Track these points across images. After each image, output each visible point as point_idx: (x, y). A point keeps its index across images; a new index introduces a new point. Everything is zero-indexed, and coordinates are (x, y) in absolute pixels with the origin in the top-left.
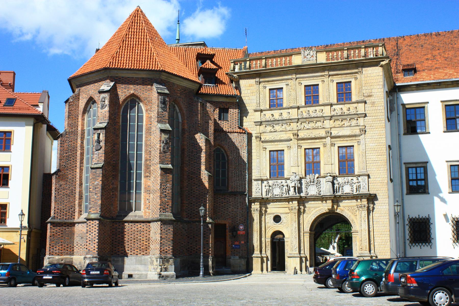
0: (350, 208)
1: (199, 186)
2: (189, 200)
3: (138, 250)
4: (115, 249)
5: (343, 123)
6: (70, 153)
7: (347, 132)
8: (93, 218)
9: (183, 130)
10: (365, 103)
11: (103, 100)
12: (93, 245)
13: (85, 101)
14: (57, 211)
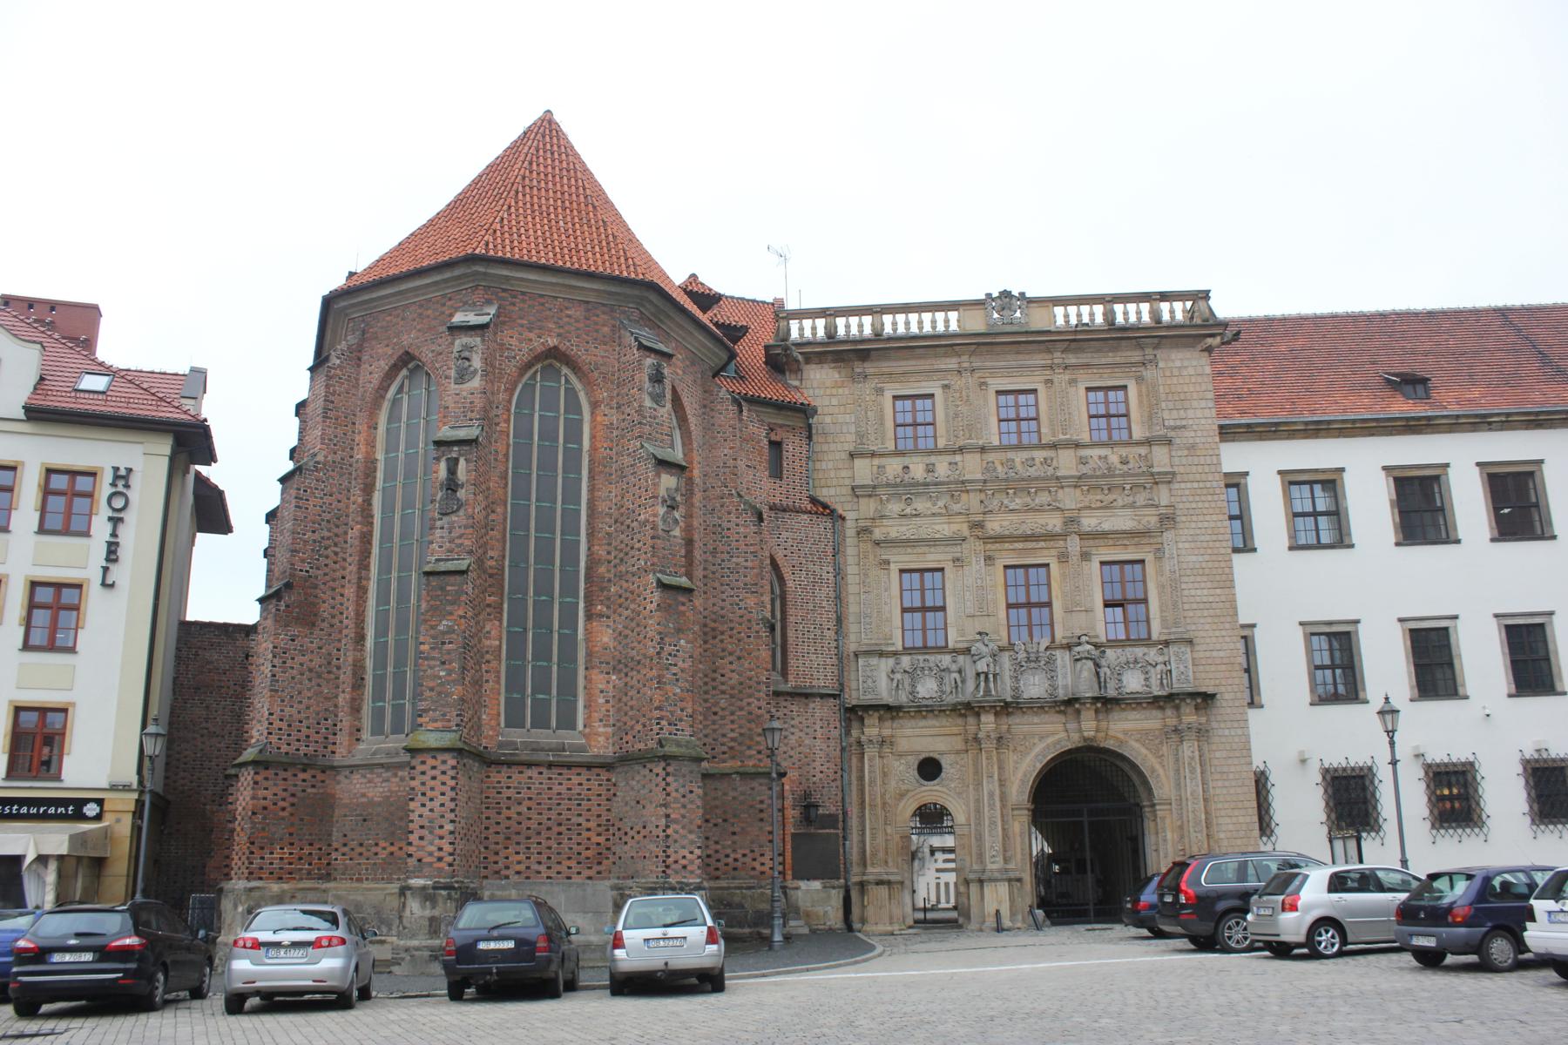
0: (1144, 736)
1: (739, 658)
3: (573, 863)
5: (1111, 497)
6: (326, 534)
7: (1122, 521)
8: (434, 745)
10: (1169, 442)
11: (466, 354)
12: (437, 841)
13: (384, 365)
14: (277, 724)
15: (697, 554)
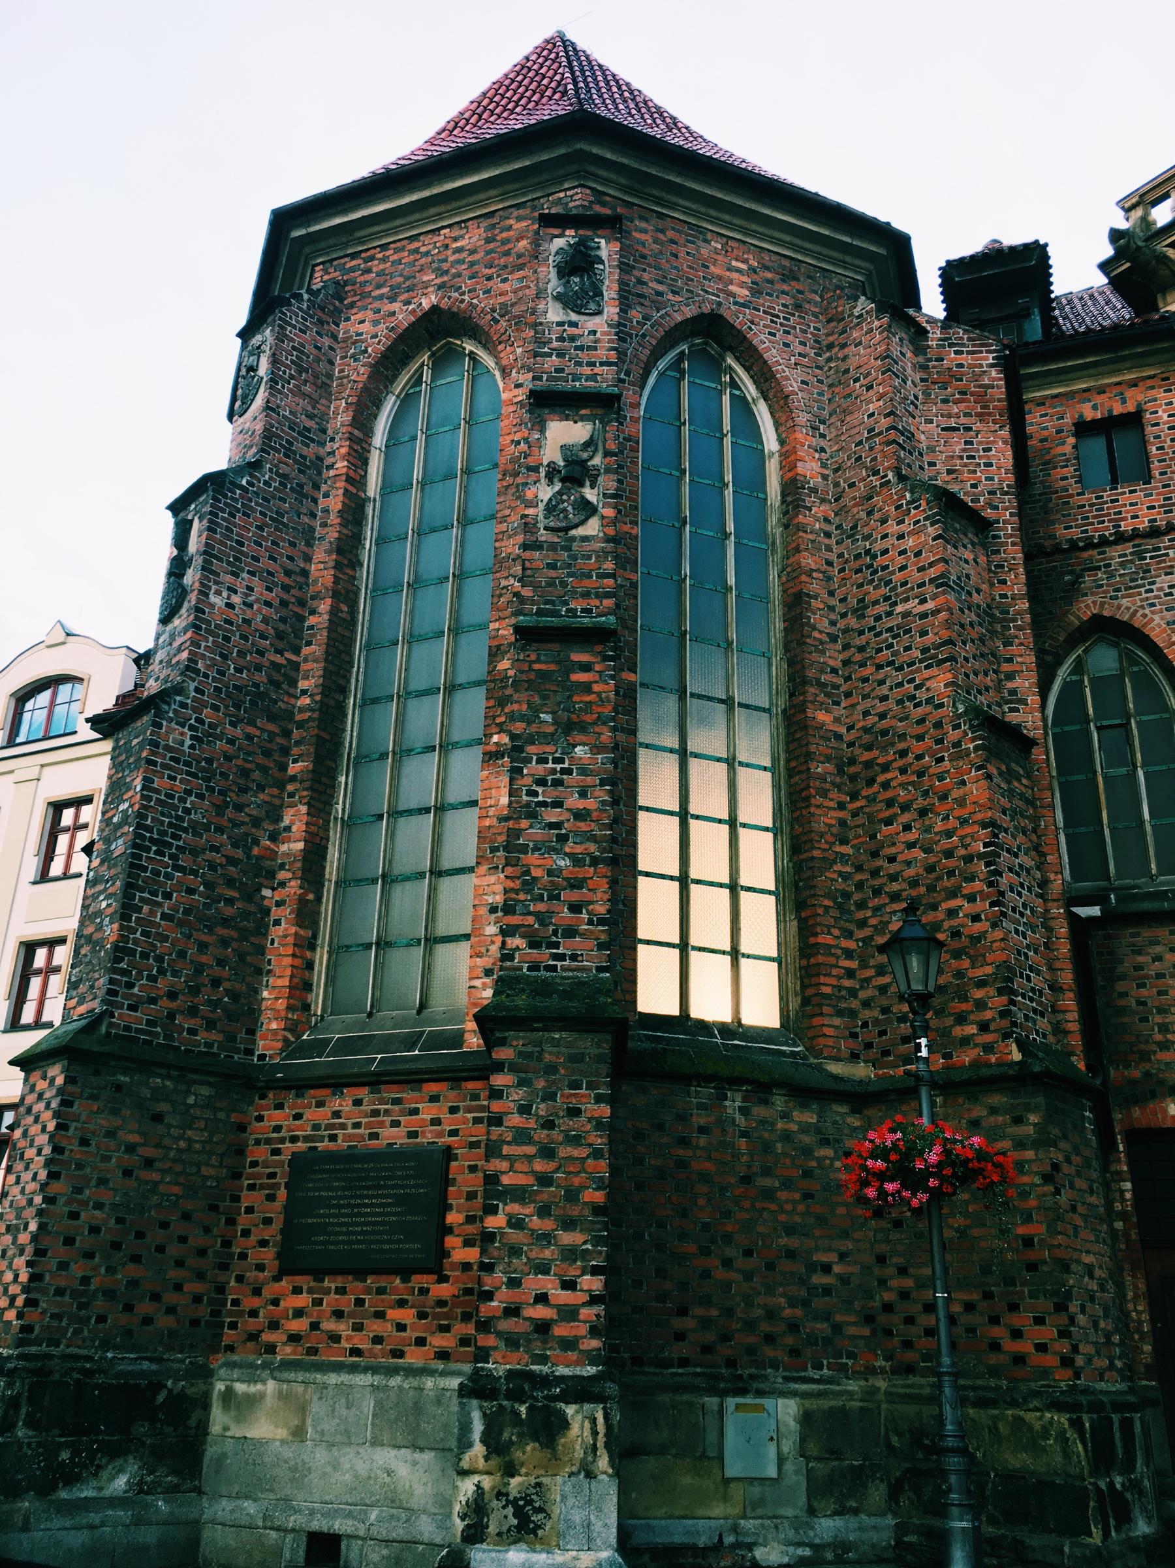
1: (923, 812)
2: (863, 924)
3: (407, 1316)
4: (256, 1302)
9: (792, 488)
15: (820, 621)
